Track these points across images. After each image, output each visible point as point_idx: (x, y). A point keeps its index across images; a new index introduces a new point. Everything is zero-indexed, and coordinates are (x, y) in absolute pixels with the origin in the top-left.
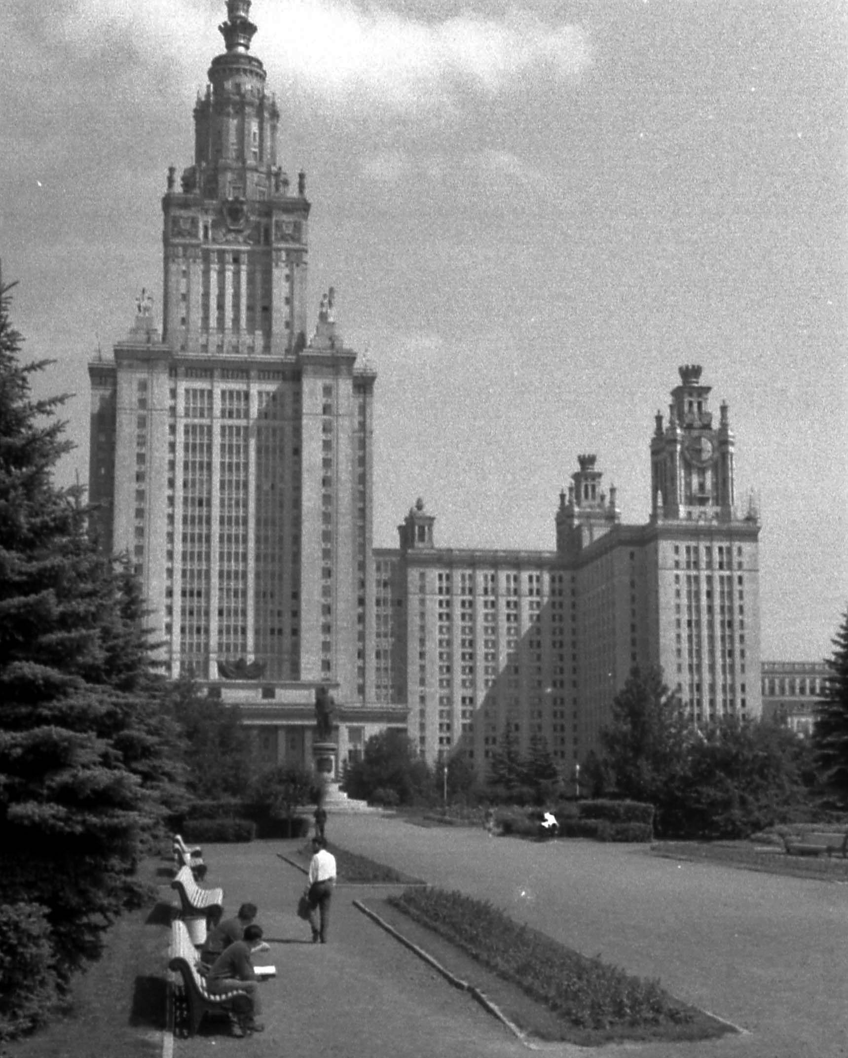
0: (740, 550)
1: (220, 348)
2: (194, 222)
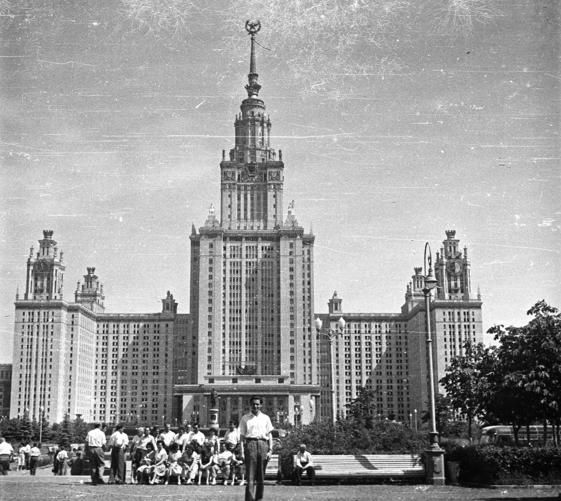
0: (473, 313)
1: (245, 227)
2: (233, 174)
